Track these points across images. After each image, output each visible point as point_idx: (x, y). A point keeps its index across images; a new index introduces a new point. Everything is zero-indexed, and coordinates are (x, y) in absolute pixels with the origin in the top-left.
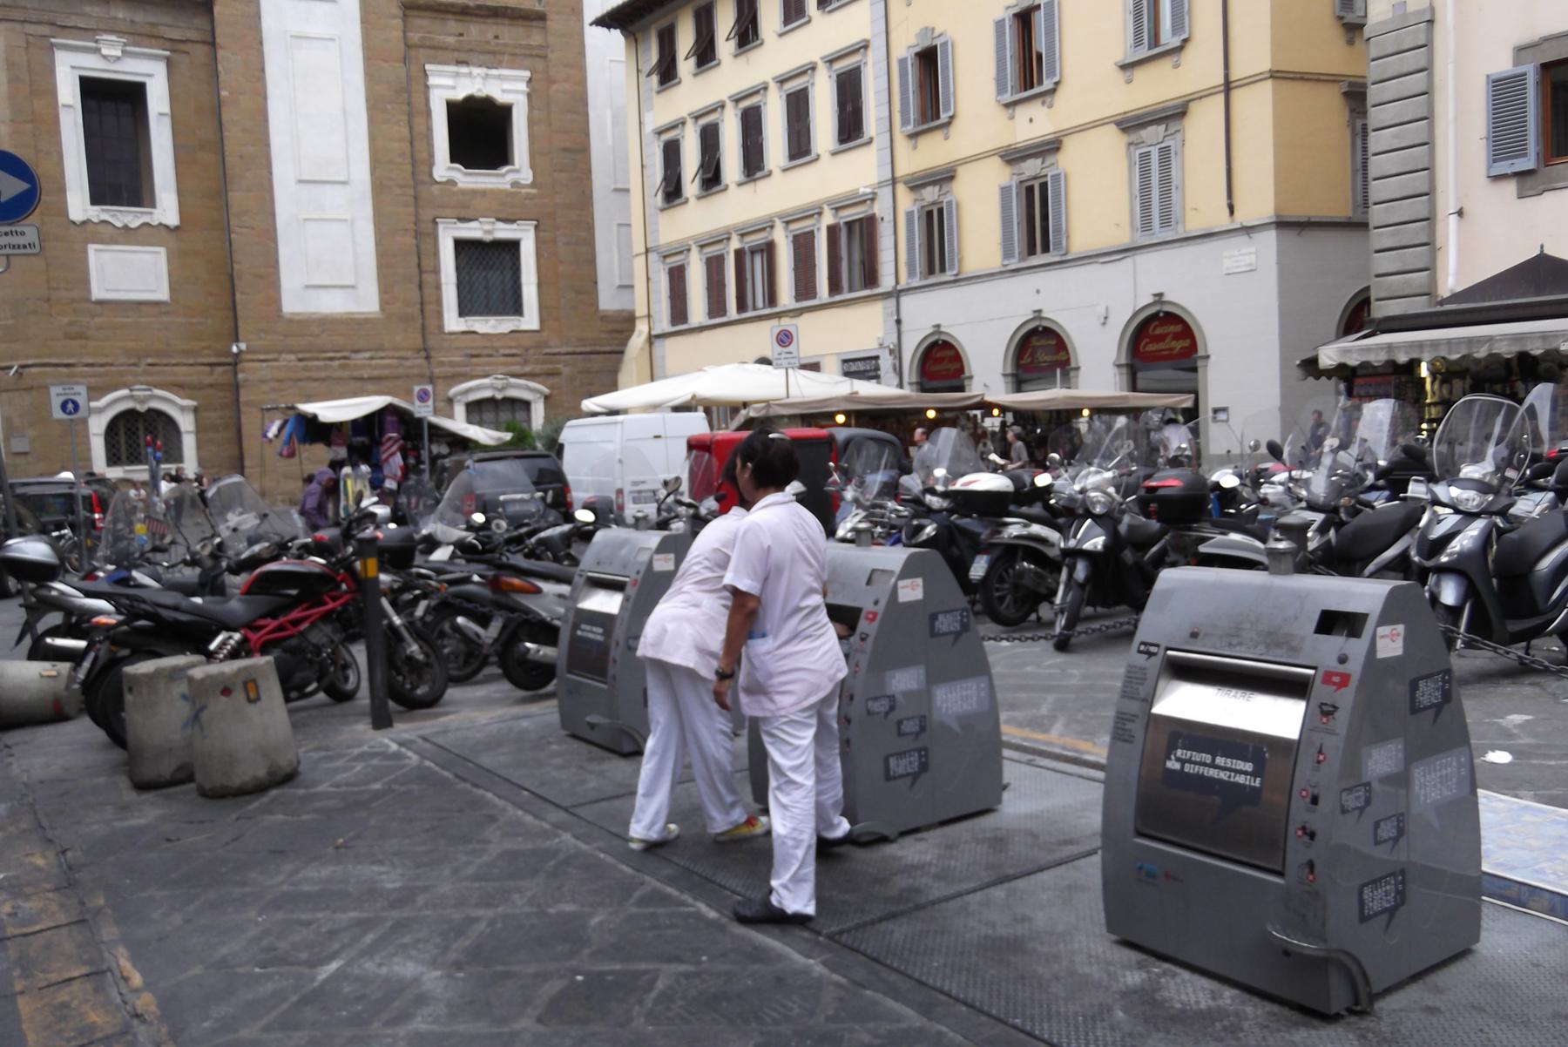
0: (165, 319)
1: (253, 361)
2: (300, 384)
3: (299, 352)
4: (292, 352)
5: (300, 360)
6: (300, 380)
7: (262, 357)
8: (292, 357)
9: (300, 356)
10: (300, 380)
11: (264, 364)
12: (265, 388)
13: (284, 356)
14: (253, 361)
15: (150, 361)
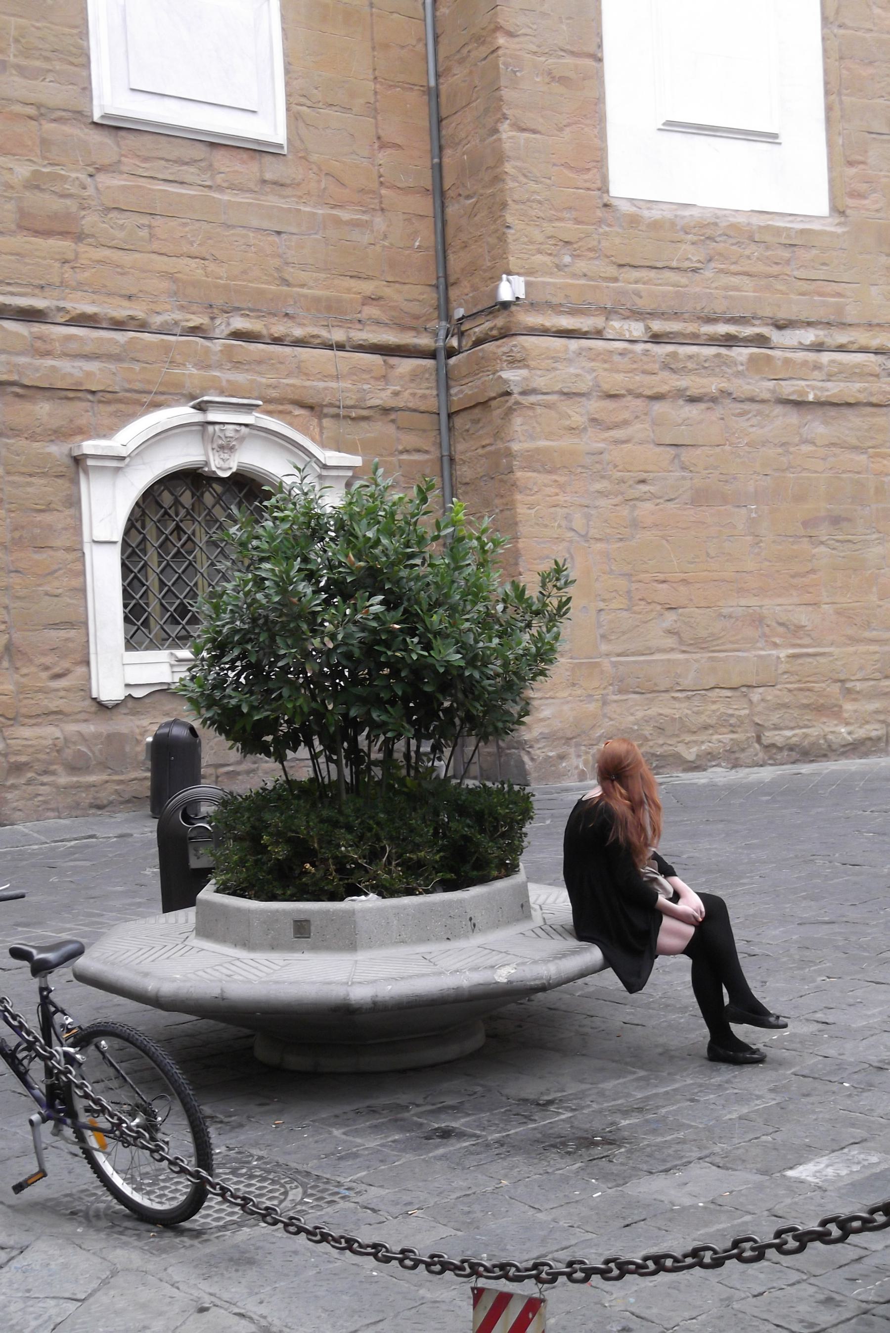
0: (272, 200)
1: (544, 332)
2: (658, 407)
3: (653, 315)
4: (636, 314)
5: (656, 338)
6: (657, 397)
7: (566, 322)
8: (636, 329)
9: (657, 326)
10: (657, 397)
11: (574, 345)
12: (577, 414)
13: (616, 325)
14: (544, 332)
15: (239, 323)
